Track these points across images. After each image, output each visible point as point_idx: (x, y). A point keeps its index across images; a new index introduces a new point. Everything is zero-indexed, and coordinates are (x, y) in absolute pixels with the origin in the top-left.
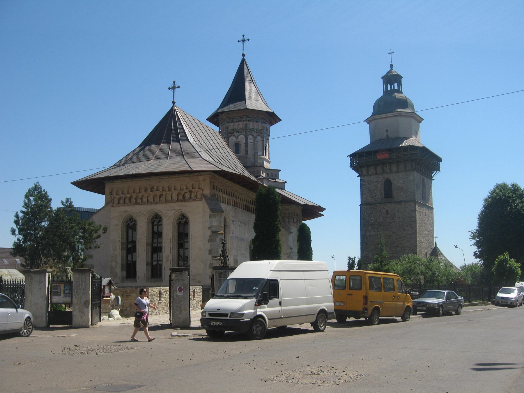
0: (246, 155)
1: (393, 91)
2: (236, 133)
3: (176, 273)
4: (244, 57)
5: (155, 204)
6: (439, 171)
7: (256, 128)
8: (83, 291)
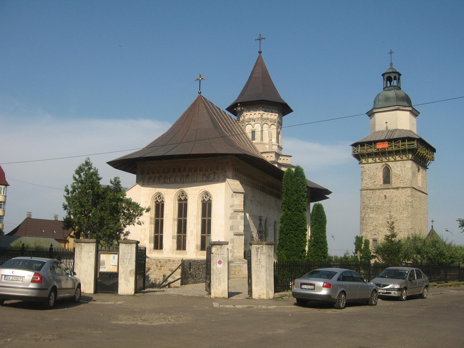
0: (261, 142)
2: (253, 121)
3: (216, 247)
4: (260, 55)
5: (182, 183)
8: (129, 261)
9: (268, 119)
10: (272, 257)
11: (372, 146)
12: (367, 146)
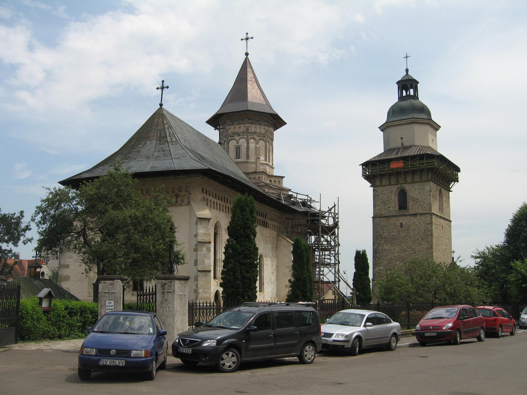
0: (247, 160)
1: (408, 97)
2: (237, 136)
3: (106, 283)
4: (247, 57)
6: (458, 181)
7: (258, 131)
9: (255, 133)
10: (186, 296)
11: (385, 166)
12: (379, 165)
